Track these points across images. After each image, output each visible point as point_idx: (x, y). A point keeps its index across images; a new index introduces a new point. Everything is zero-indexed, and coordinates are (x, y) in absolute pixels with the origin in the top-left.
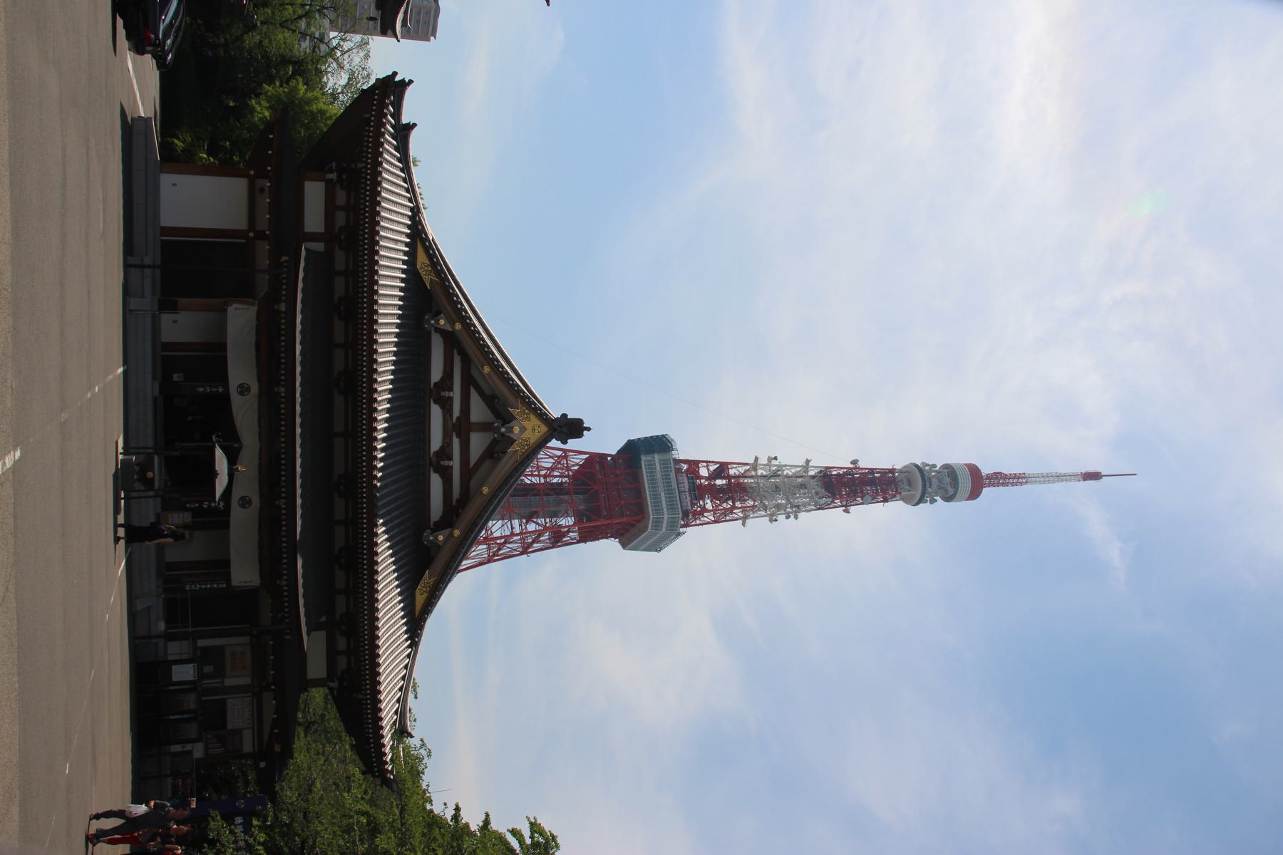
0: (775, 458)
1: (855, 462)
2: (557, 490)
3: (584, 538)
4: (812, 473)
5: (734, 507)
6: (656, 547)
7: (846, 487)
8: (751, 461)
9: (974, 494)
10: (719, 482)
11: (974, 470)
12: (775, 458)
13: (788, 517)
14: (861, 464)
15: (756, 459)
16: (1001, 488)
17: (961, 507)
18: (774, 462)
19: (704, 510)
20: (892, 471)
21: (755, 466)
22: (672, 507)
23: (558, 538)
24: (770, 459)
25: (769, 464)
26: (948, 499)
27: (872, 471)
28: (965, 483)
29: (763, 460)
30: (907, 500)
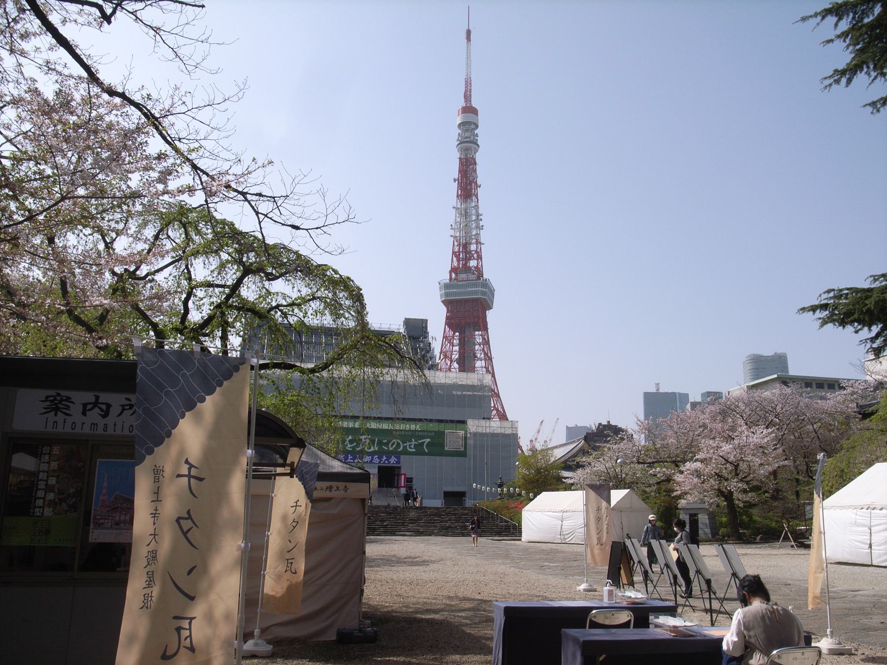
1: (455, 180)
2: (462, 344)
3: (485, 328)
5: (476, 251)
6: (492, 292)
7: (467, 186)
8: (452, 239)
9: (474, 111)
14: (456, 177)
16: (472, 94)
17: (482, 119)
19: (477, 267)
20: (460, 159)
21: (455, 237)
22: (476, 285)
23: (486, 342)
25: (454, 229)
26: (477, 126)
27: (460, 171)
28: (470, 117)
29: (452, 232)
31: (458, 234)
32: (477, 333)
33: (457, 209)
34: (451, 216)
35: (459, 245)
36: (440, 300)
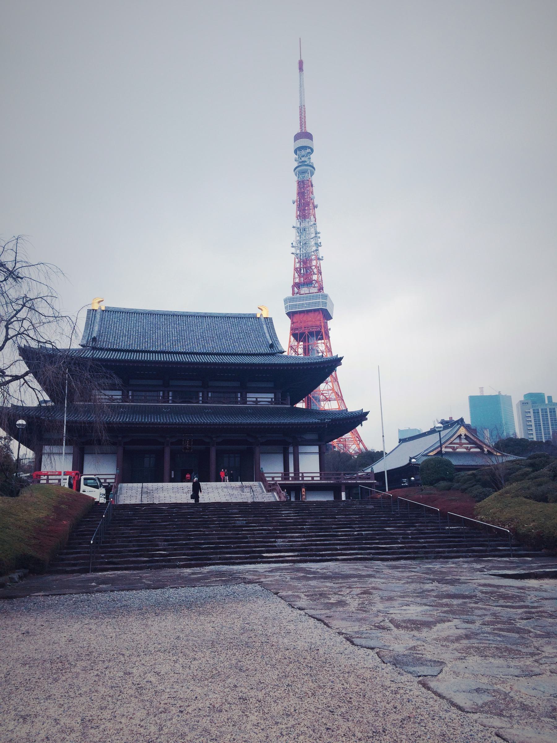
0: (292, 244)
3: (328, 337)
4: (298, 226)
7: (305, 206)
8: (293, 256)
9: (309, 136)
10: (302, 272)
11: (297, 137)
12: (292, 244)
13: (319, 238)
15: (293, 253)
17: (316, 144)
18: (294, 245)
20: (299, 182)
24: (293, 247)
30: (312, 174)
31: (298, 252)
32: (319, 341)
33: (298, 228)
34: (292, 236)
35: (300, 262)
36: (285, 313)
